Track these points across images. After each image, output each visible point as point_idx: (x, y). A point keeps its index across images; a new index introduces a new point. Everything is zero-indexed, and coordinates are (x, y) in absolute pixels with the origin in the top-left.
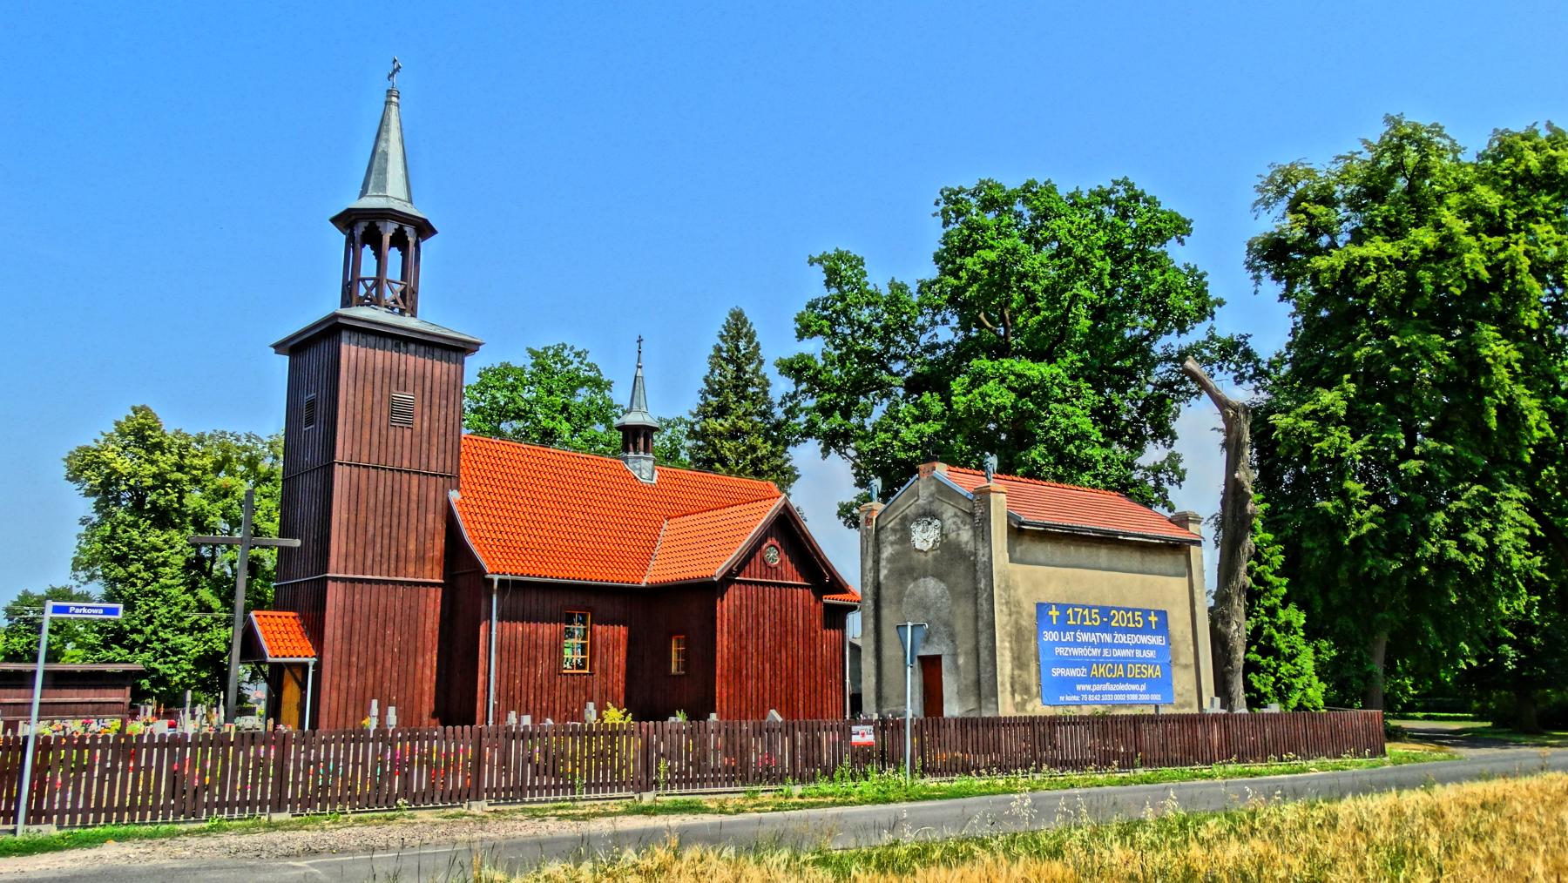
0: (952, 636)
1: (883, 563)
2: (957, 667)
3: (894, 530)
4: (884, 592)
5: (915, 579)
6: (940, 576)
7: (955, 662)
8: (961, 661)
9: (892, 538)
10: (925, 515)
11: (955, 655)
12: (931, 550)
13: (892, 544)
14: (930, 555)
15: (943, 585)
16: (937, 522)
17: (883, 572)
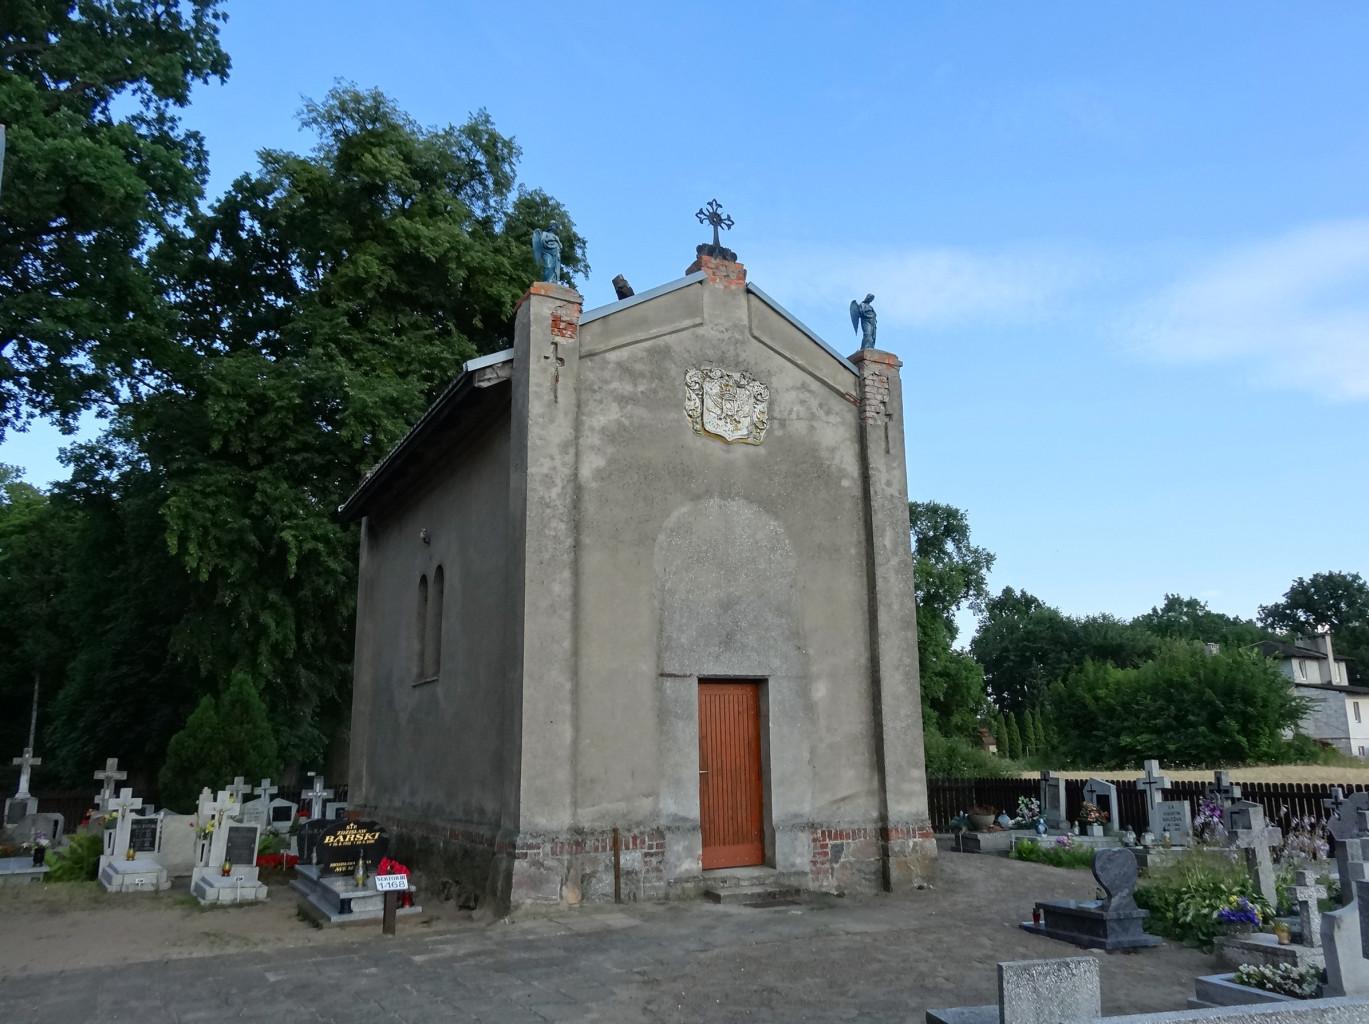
0: (797, 637)
1: (591, 439)
2: (810, 708)
3: (625, 370)
4: (590, 507)
5: (697, 498)
6: (768, 505)
7: (804, 692)
8: (820, 691)
9: (627, 388)
10: (722, 361)
11: (804, 681)
12: (742, 441)
13: (622, 400)
14: (739, 452)
15: (773, 524)
16: (756, 387)
17: (591, 464)
